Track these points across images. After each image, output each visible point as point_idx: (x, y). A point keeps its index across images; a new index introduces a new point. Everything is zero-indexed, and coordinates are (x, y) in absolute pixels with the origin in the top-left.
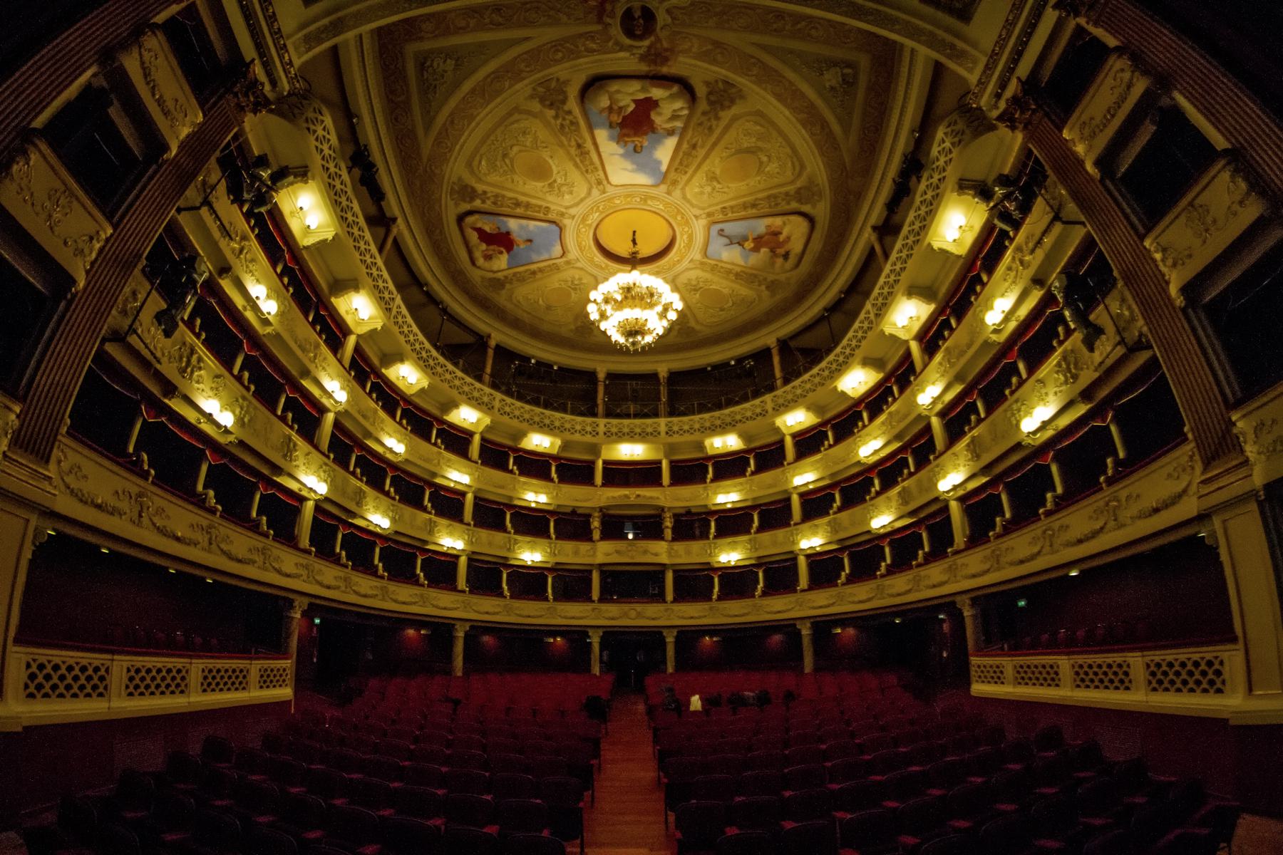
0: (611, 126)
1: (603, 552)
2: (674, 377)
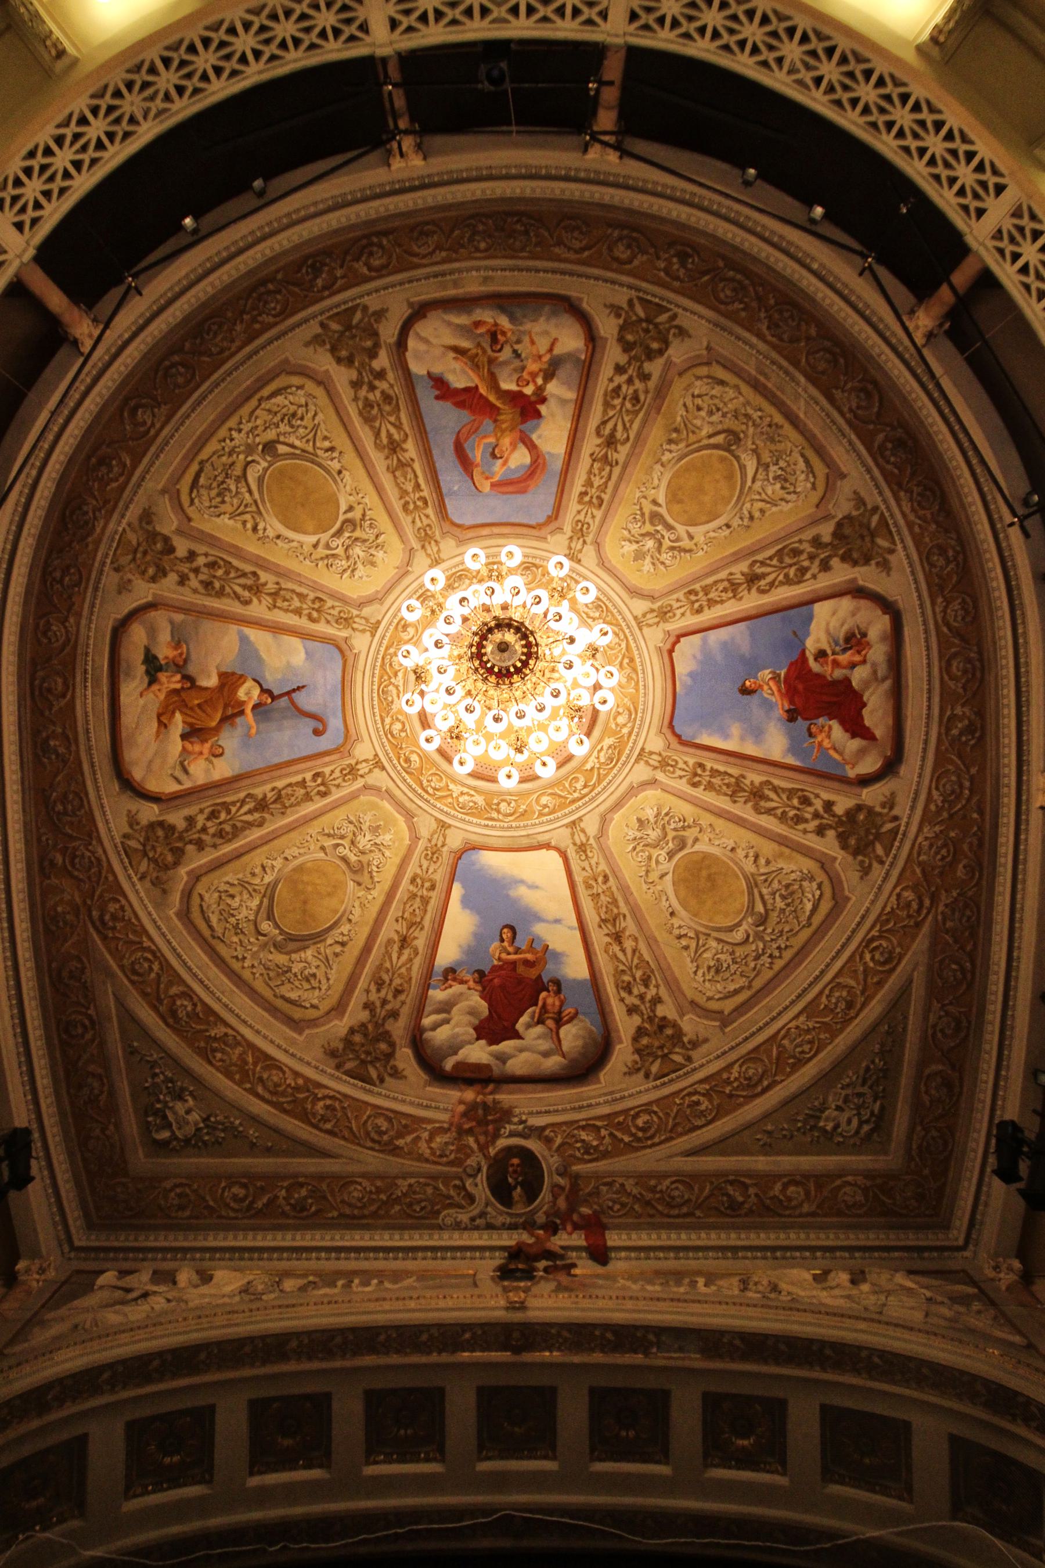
0: (557, 983)
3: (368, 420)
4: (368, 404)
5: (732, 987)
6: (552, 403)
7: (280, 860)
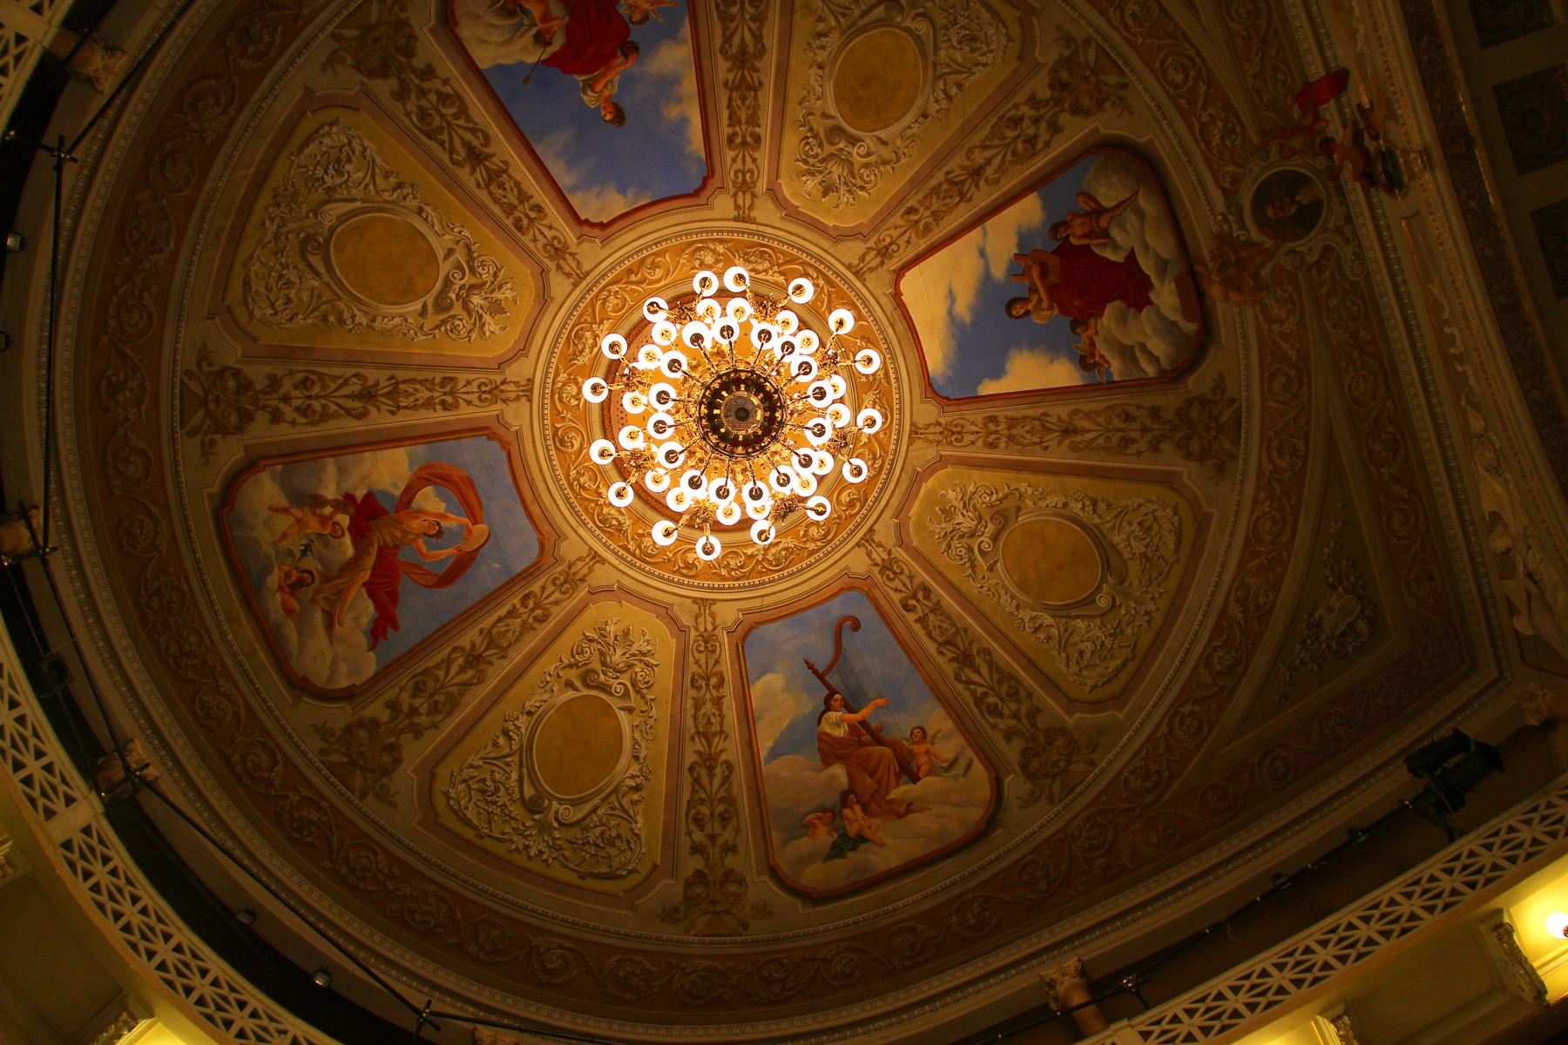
0: (1055, 229)
3: (454, 703)
4: (435, 709)
5: (986, 16)
6: (348, 486)
7: (1021, 614)
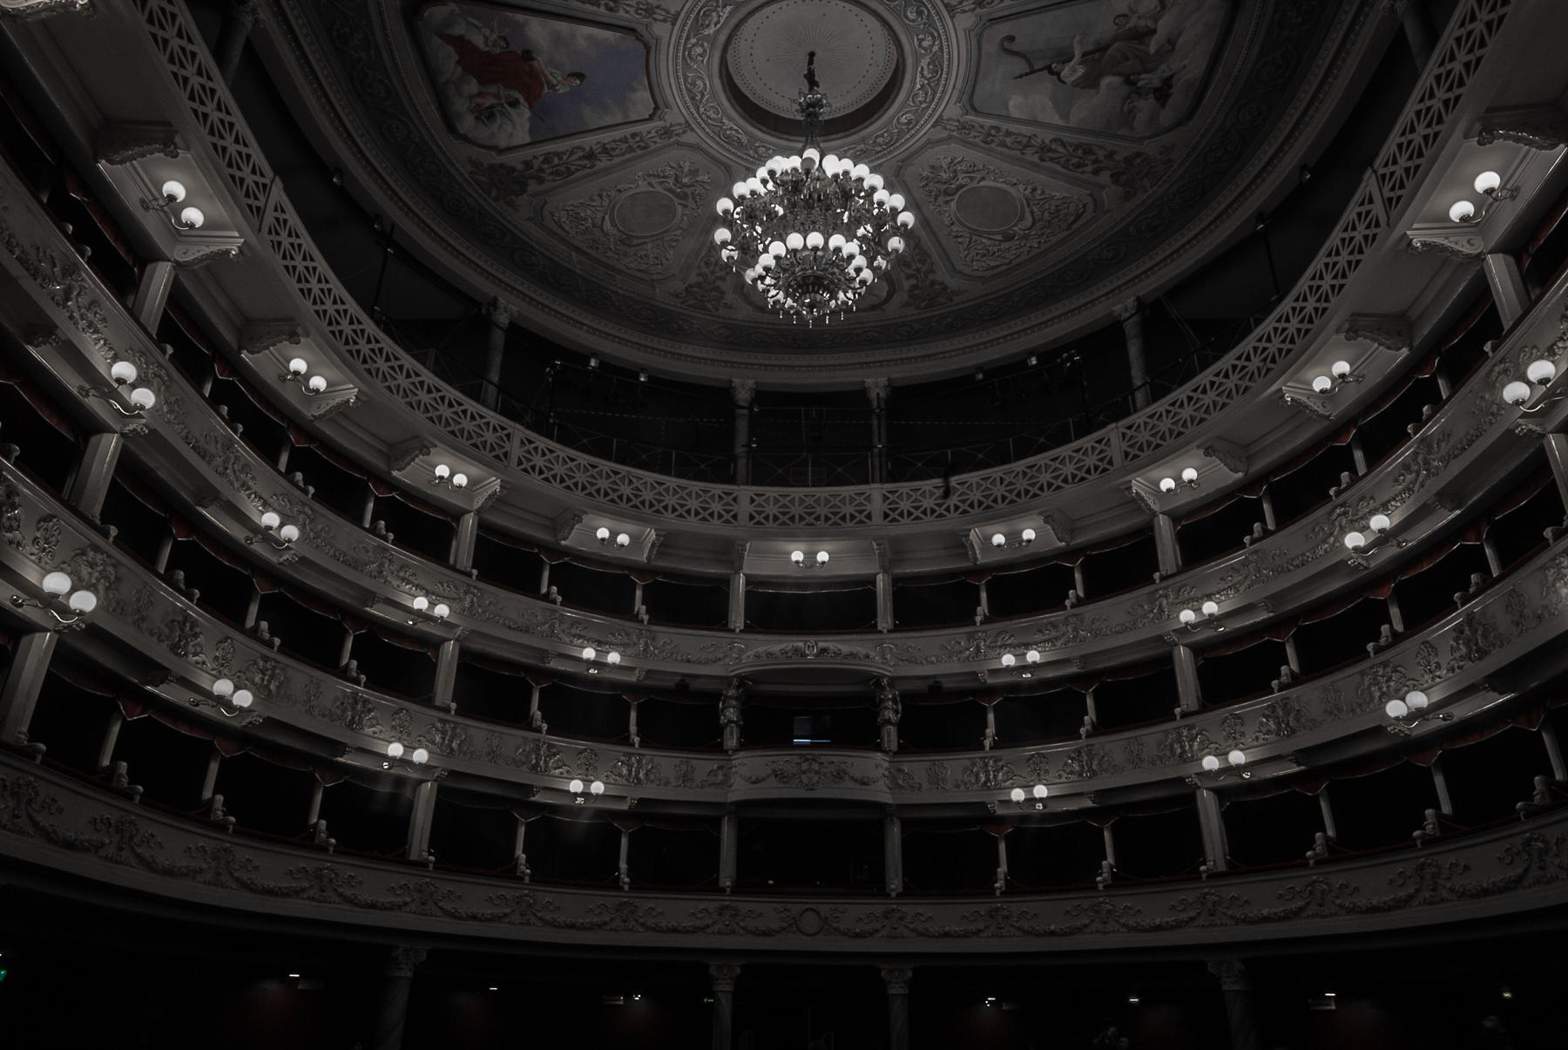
1: (747, 775)
2: (901, 395)
